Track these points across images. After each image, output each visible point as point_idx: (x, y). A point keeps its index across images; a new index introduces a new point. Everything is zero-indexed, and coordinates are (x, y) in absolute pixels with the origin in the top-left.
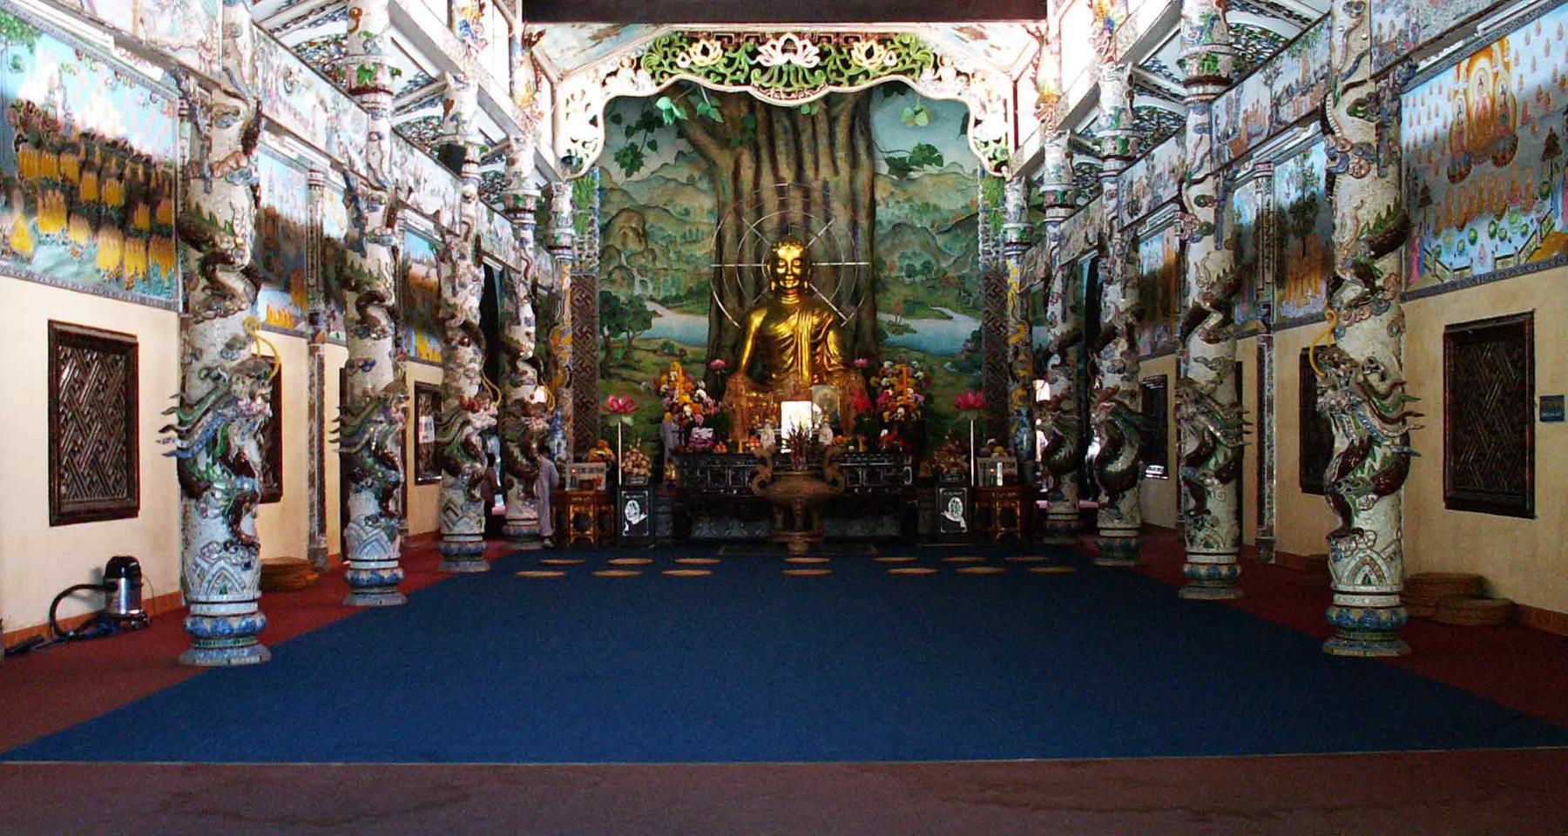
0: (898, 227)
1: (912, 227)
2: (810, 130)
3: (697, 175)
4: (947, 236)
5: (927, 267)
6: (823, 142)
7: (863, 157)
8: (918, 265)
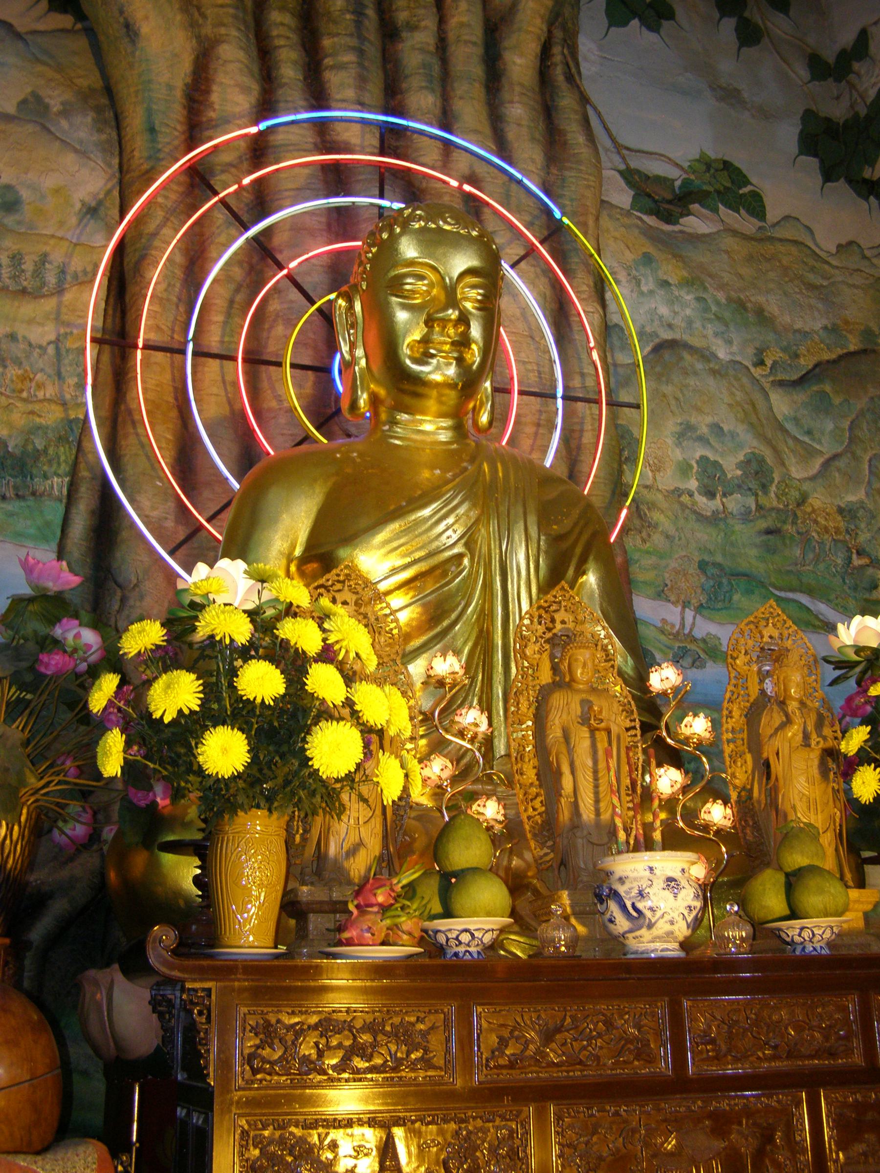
0: (665, 351)
1: (706, 355)
2: (430, 23)
3: (55, 99)
4: (801, 396)
5: (757, 473)
6: (467, 58)
7: (576, 137)
8: (731, 465)
